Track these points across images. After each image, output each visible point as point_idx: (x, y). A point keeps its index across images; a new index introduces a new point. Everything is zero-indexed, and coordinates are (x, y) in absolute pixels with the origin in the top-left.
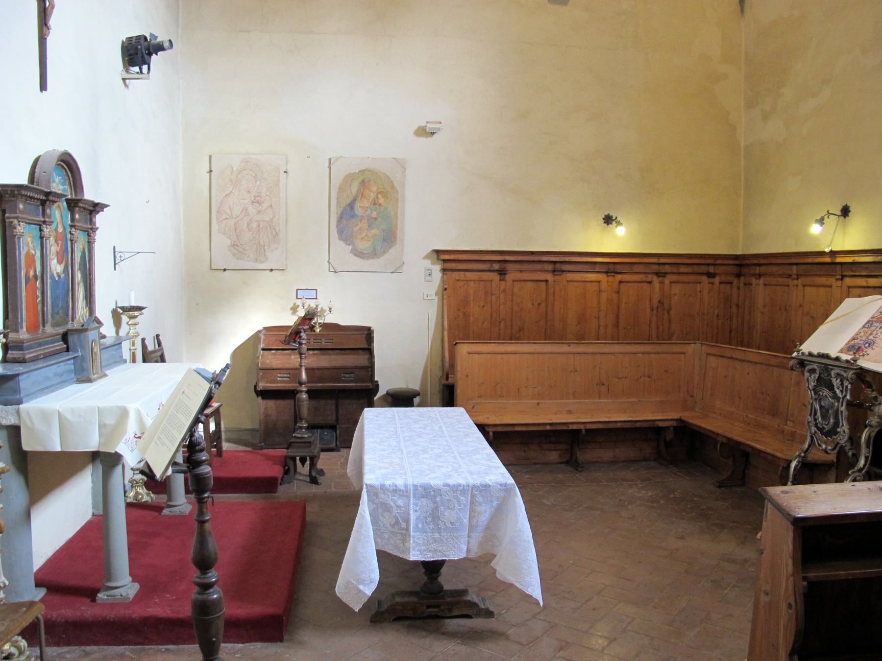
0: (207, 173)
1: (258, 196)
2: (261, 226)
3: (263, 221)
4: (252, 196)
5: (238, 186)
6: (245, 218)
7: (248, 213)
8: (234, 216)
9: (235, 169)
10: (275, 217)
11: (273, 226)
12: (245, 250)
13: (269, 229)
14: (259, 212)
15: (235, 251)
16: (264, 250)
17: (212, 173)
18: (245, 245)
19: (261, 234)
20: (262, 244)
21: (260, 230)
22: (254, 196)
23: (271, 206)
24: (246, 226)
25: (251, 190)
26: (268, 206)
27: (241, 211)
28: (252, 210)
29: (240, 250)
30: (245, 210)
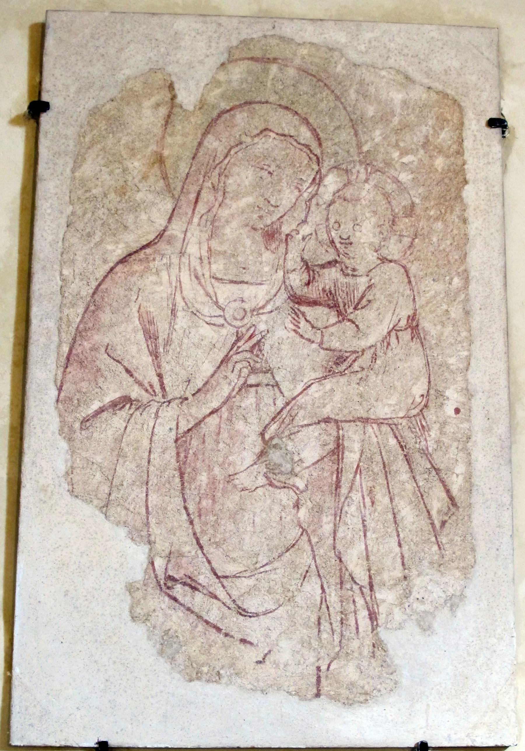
0: (15, 121)
1: (331, 264)
3: (366, 421)
7: (269, 371)
10: (440, 394)
11: (425, 453)
12: (242, 612)
13: (401, 465)
16: (373, 616)
17: (45, 118)
18: (245, 583)
20: (362, 578)
21: (346, 477)
22: (307, 266)
24: (249, 457)
25: (285, 229)
26: (395, 329)
27: (221, 356)
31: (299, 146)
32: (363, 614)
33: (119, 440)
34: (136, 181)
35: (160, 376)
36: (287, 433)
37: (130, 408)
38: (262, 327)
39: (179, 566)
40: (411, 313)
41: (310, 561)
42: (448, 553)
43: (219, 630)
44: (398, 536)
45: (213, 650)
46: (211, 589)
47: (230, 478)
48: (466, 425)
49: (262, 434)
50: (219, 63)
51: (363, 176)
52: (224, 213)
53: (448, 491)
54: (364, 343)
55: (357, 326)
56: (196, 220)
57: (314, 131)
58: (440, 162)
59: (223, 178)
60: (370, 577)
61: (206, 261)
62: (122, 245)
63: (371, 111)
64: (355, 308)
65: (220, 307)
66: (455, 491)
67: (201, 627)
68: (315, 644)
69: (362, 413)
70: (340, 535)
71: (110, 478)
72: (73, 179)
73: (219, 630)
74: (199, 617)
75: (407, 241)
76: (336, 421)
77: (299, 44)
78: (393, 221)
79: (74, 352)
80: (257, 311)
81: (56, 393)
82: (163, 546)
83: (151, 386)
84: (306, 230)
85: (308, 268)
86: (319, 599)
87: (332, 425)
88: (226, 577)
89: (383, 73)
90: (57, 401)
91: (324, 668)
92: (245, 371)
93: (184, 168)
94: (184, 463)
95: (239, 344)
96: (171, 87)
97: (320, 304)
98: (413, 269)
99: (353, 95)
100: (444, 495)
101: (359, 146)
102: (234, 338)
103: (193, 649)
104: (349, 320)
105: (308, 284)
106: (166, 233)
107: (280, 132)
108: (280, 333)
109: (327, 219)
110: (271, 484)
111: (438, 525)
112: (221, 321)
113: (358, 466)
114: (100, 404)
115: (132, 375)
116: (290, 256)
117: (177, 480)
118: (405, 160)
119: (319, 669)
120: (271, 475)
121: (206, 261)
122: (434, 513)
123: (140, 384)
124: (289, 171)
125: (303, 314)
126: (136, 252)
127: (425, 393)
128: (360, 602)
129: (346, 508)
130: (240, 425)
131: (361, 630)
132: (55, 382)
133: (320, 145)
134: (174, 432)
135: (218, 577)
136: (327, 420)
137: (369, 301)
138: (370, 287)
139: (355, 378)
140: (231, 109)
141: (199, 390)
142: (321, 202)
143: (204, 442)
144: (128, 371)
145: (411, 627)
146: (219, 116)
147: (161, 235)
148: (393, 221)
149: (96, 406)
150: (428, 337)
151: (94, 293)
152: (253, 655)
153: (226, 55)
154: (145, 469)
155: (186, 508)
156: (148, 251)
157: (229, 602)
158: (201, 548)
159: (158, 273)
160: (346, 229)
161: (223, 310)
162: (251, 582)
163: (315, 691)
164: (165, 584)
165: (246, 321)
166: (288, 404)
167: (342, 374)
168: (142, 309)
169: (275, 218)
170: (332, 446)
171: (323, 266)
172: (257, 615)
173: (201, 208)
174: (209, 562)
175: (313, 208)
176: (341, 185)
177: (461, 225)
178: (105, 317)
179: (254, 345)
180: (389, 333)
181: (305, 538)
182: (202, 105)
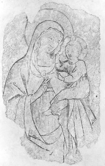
1: (66, 61)
2: (71, 108)
3: (74, 99)
4: (57, 61)
5: (36, 45)
6: (47, 94)
8: (29, 93)
9: (31, 20)
11: (89, 107)
12: (47, 144)
13: (82, 109)
14: (69, 85)
15: (32, 146)
16: (76, 144)
19: (71, 120)
21: (70, 112)
23: (86, 76)
25: (55, 53)
28: (57, 84)
29: (40, 144)
30: (46, 83)
31: (58, 32)
32: (74, 144)
33: (17, 105)
34: (19, 42)
35: (26, 89)
36: (56, 102)
37: (20, 97)
38: (50, 77)
39: (31, 133)
40: (86, 73)
41: (62, 132)
42: (94, 130)
43: (41, 147)
44: (82, 126)
45: (40, 152)
46: (39, 138)
47: (43, 113)
48: (98, 100)
49: (50, 103)
50: (39, 10)
51: (74, 39)
52: (40, 49)
53: (94, 115)
54: (74, 81)
55: (73, 76)
56: (34, 51)
57: (62, 27)
58: (94, 34)
59: (40, 41)
60: (76, 136)
61: (36, 62)
62: (16, 58)
63: (76, 21)
64: (72, 72)
65: (40, 73)
66: (96, 116)
67: (37, 147)
68: (63, 150)
69: (74, 97)
70: (68, 126)
71: (15, 113)
72: (4, 42)
73: (41, 147)
74: (37, 145)
75: (85, 55)
76: (68, 99)
77: (58, 4)
78: (82, 50)
79: (6, 84)
80: (49, 73)
81: (3, 94)
82: (28, 129)
83: (24, 92)
84: (60, 53)
85: (61, 63)
86: (64, 140)
87: (67, 100)
88: (43, 136)
89: (79, 11)
90: (3, 96)
91: (65, 156)
92: (46, 88)
93: (30, 38)
94: (32, 110)
95: (45, 81)
96: (27, 18)
97: (64, 71)
98: (86, 62)
99: (72, 17)
100: (93, 116)
101: (73, 31)
102: (43, 80)
103: (36, 152)
104: (71, 75)
105: (61, 67)
106: (27, 55)
107: (54, 28)
108: (54, 79)
109: (65, 50)
110: (52, 114)
111: (91, 123)
112: (40, 76)
113: (73, 110)
114: (13, 97)
115: (20, 89)
116: (56, 60)
117: (31, 114)
118: (85, 34)
119: (64, 156)
120: (52, 112)
121: (36, 62)
122: (91, 121)
123: (22, 91)
124: (56, 38)
125: (60, 74)
126: (20, 60)
127: (89, 92)
128: (73, 141)
129: (70, 119)
130: (45, 101)
131: (73, 147)
132: (2, 91)
133: (64, 31)
134: (30, 102)
135: (41, 136)
136: (65, 99)
137: (76, 70)
138: (76, 67)
139: (72, 89)
140: (42, 23)
141: (35, 93)
142: (64, 46)
143: (37, 105)
144: (19, 88)
145: (85, 147)
146: (39, 25)
147: (25, 55)
148: (82, 50)
149: (12, 97)
150: (90, 79)
151: (10, 70)
152: (49, 153)
153: (40, 9)
154: (23, 111)
155: (33, 120)
156: (23, 59)
157: (43, 141)
158: (37, 129)
159: (25, 65)
160: (70, 53)
161: (41, 73)
162: (48, 137)
163: (63, 161)
164: (29, 137)
165: (46, 76)
166: (56, 95)
167: (69, 88)
168: (22, 74)
169: (52, 50)
170: (67, 105)
171: (64, 62)
172: (50, 144)
173: (35, 48)
174: (39, 132)
175: (62, 47)
176: (69, 41)
177: (98, 50)
178: (13, 76)
179: (48, 82)
180: (80, 78)
181: (60, 126)
182: (34, 22)
